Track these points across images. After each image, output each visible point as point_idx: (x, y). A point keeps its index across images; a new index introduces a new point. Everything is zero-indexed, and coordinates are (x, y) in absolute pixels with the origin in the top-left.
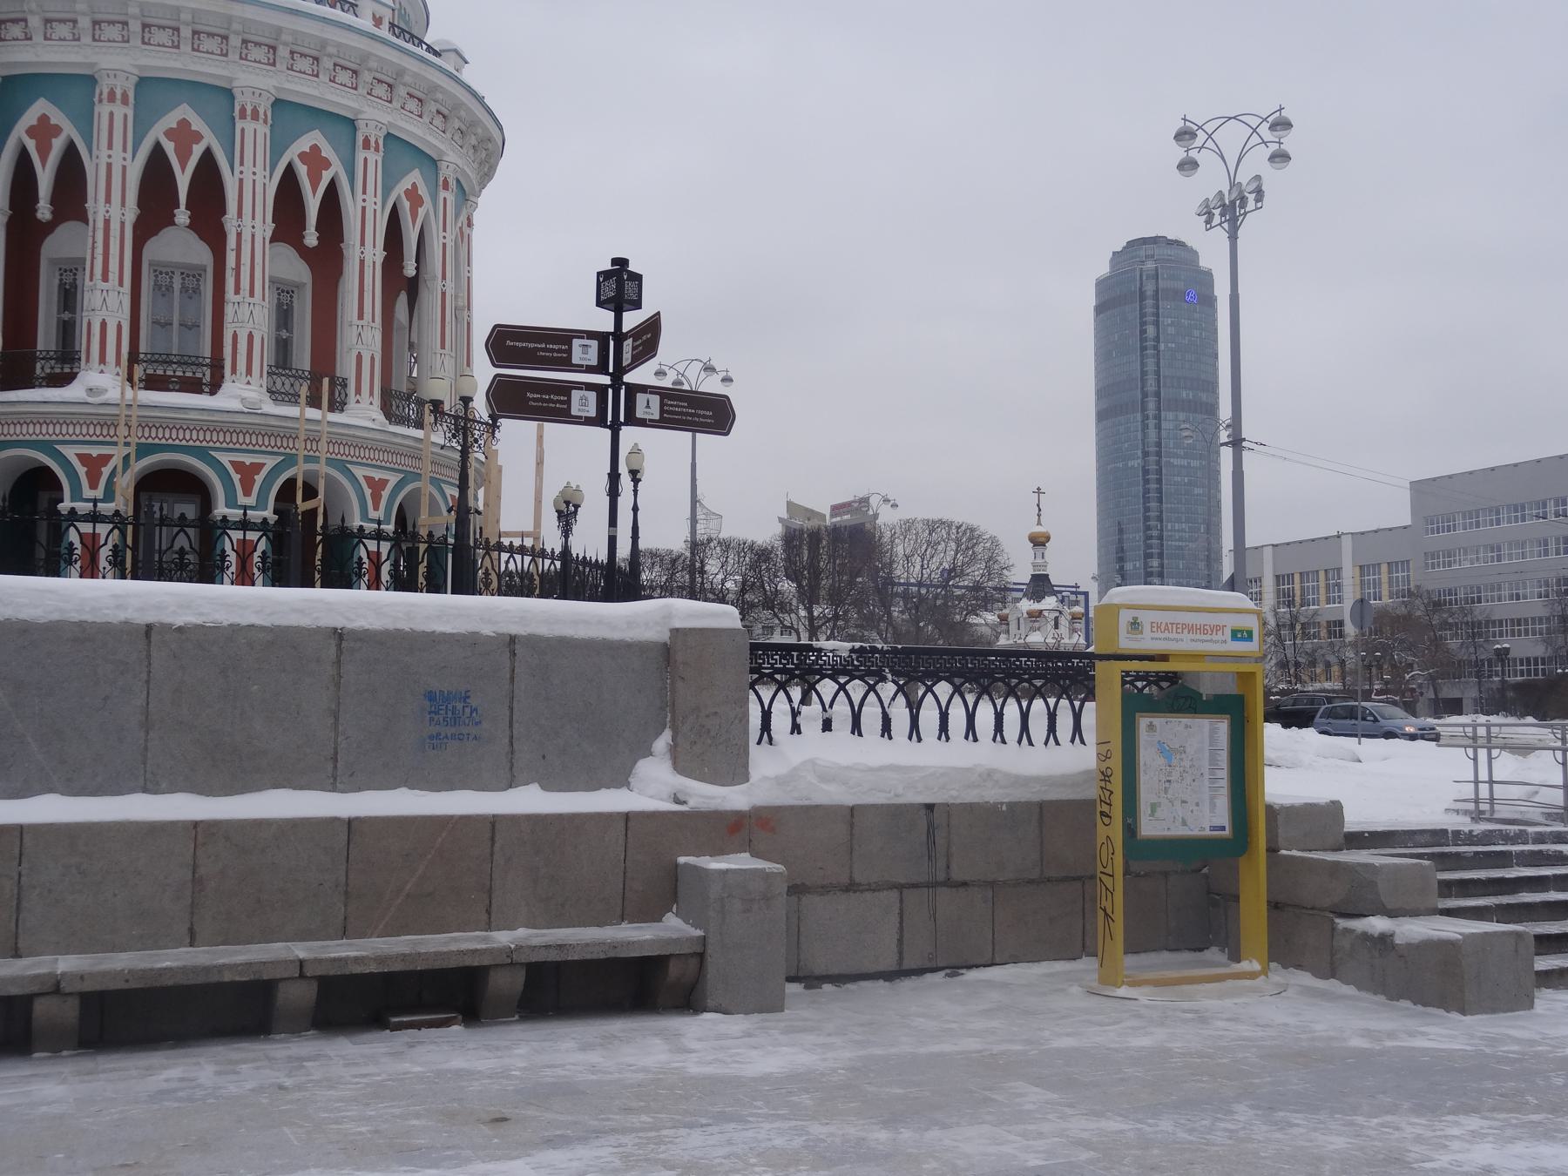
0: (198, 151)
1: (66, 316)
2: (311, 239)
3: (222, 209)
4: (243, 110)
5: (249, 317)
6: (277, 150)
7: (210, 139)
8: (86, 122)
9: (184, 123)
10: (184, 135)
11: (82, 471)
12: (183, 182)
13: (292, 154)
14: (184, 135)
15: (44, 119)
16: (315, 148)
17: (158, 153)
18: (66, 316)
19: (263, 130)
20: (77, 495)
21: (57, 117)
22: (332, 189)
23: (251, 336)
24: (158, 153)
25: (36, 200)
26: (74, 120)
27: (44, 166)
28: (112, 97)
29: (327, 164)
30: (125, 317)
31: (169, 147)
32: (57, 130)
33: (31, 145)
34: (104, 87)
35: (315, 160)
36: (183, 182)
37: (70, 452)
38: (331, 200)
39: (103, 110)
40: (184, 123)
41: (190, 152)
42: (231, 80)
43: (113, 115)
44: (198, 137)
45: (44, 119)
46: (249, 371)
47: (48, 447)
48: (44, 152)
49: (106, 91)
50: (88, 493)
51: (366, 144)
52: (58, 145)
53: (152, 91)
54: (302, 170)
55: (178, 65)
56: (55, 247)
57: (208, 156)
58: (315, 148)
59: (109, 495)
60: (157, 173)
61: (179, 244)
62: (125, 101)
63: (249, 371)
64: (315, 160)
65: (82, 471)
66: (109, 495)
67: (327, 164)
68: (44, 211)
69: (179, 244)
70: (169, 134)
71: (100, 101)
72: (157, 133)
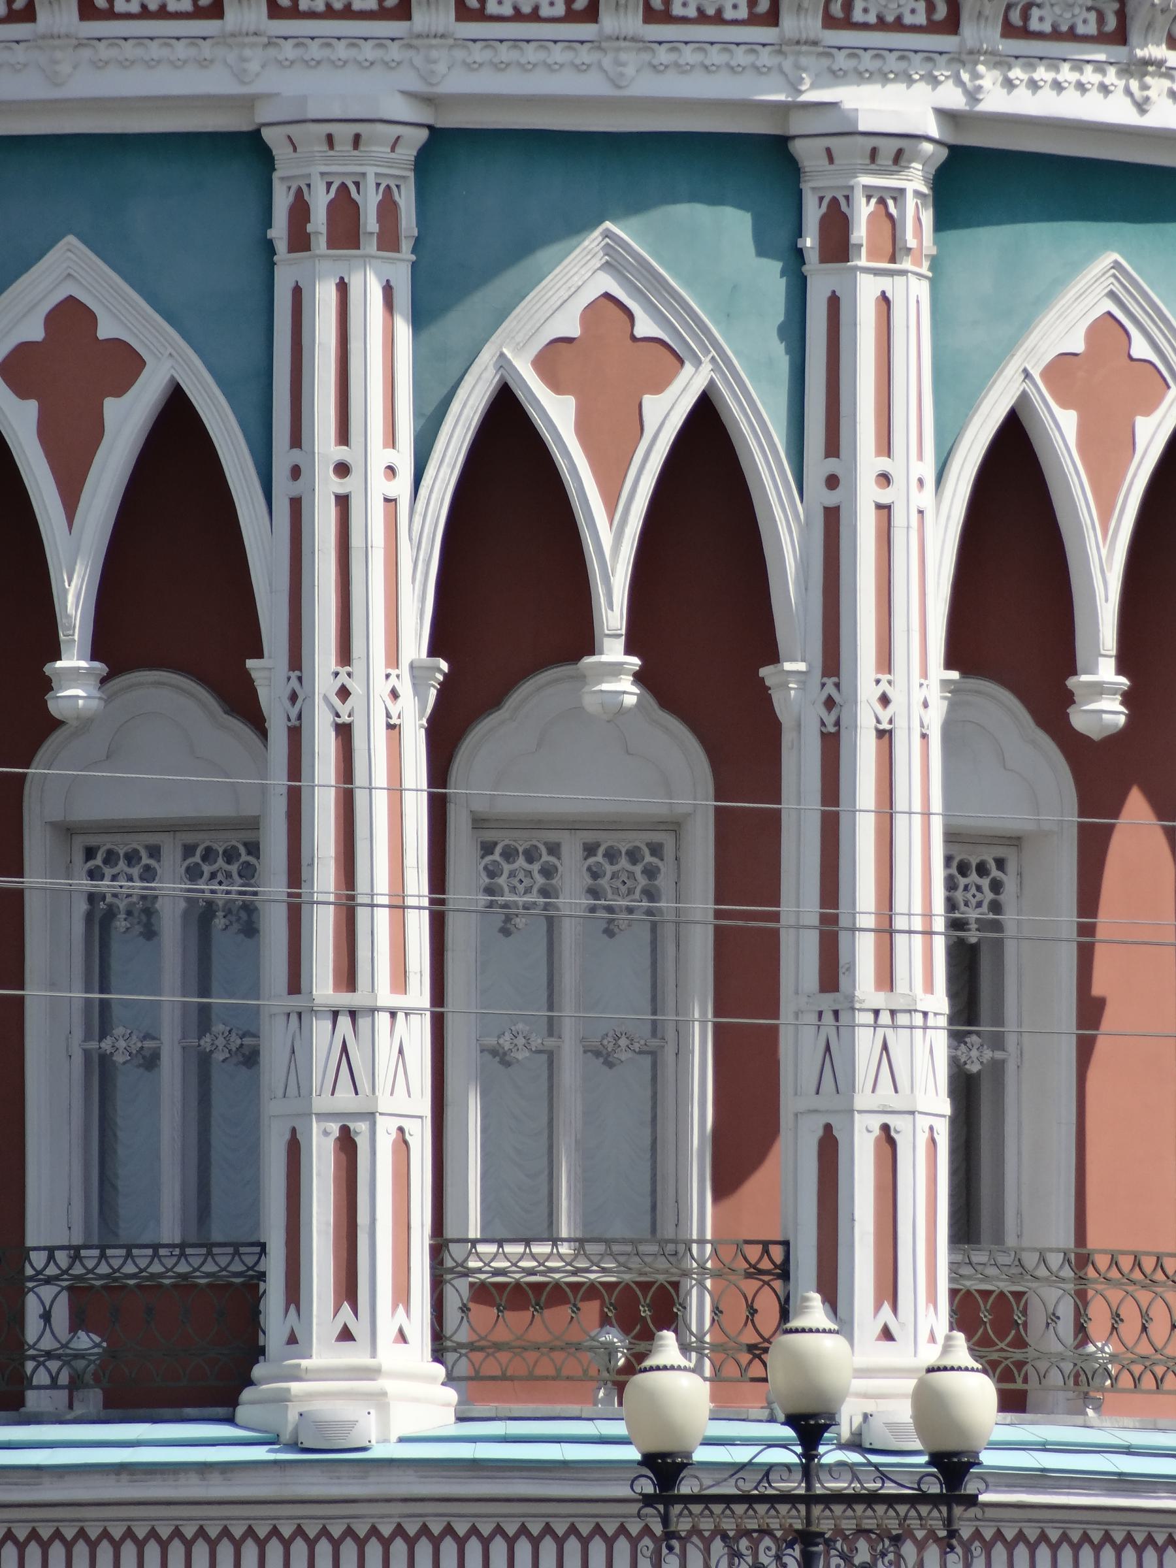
12: (613, 544)
15: (71, 317)
17: (507, 416)
21: (120, 315)
24: (507, 416)
27: (71, 499)
28: (345, 230)
31: (557, 414)
32: (124, 364)
36: (613, 544)
45: (71, 317)
49: (320, 202)
52: (127, 420)
55: (592, 85)
70: (555, 359)
71: (300, 241)
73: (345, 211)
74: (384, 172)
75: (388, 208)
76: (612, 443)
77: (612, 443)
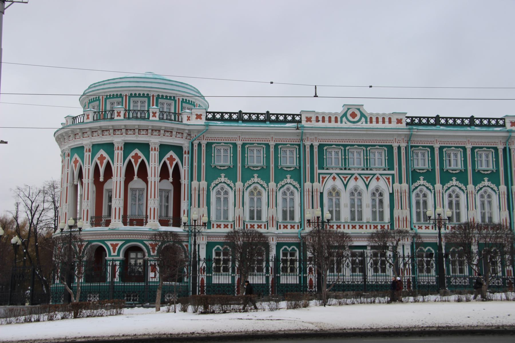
0: (140, 161)
1: (110, 204)
2: (171, 179)
3: (147, 175)
4: (152, 148)
5: (153, 203)
6: (161, 158)
7: (143, 157)
8: (111, 154)
9: (136, 154)
10: (136, 157)
11: (111, 248)
13: (165, 159)
14: (136, 157)
16: (171, 156)
17: (130, 161)
18: (110, 204)
19: (157, 153)
20: (110, 255)
22: (177, 165)
23: (154, 209)
24: (130, 161)
25: (100, 176)
26: (108, 154)
29: (174, 159)
30: (122, 205)
31: (133, 160)
32: (105, 158)
33: (98, 162)
34: (116, 146)
35: (171, 159)
37: (109, 243)
38: (177, 169)
39: (116, 152)
40: (136, 154)
41: (138, 161)
42: (149, 141)
43: (118, 153)
44: (140, 157)
45: (102, 155)
46: (154, 218)
47: (103, 241)
48: (102, 163)
50: (112, 254)
51: (185, 153)
52: (105, 162)
53: (128, 147)
54: (168, 162)
56: (106, 186)
57: (143, 161)
58: (171, 156)
59: (118, 255)
60: (130, 167)
61: (137, 183)
62: (121, 149)
63: (154, 218)
64: (171, 159)
65: (111, 248)
66: (118, 255)
67: (174, 159)
68: (101, 179)
69: (137, 183)
70: (133, 157)
72: (130, 157)
73: (118, 148)
74: (121, 145)
75: (121, 148)
76: (136, 162)
77: (136, 162)
